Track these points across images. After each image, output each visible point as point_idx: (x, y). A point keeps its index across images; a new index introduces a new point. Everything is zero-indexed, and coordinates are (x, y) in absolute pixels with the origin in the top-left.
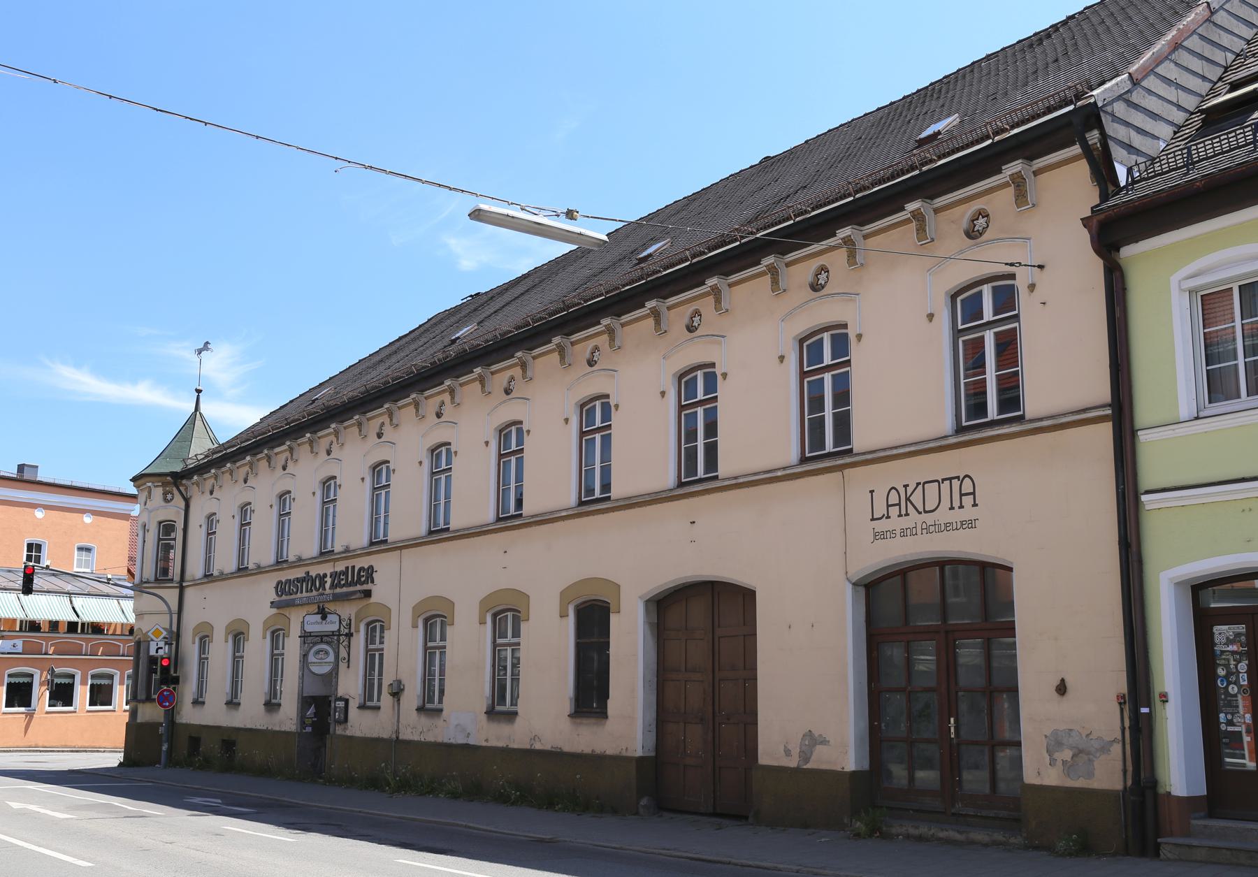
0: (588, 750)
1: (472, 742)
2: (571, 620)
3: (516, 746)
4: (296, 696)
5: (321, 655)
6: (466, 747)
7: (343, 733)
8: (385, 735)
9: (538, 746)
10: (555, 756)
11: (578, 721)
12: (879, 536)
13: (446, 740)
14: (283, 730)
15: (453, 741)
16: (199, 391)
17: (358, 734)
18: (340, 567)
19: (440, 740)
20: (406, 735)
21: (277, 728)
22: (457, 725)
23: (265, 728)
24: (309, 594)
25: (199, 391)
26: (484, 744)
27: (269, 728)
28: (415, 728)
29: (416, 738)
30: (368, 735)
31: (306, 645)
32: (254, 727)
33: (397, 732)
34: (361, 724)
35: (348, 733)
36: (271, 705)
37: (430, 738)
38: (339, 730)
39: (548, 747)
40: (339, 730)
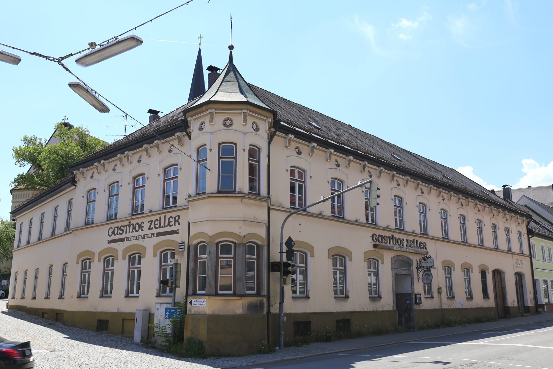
0: (487, 307)
1: (464, 307)
2: (480, 274)
3: (474, 307)
4: (392, 293)
5: (426, 276)
6: (463, 308)
7: (419, 308)
8: (437, 307)
9: (478, 307)
10: (482, 309)
11: (486, 299)
12: (516, 267)
13: (457, 308)
14: (385, 310)
15: (459, 307)
16: (231, 48)
17: (426, 308)
18: (411, 238)
19: (455, 307)
20: (444, 307)
21: (381, 309)
22: (459, 302)
23: (371, 310)
24: (394, 246)
25: (231, 48)
26: (466, 307)
27: (375, 310)
28: (447, 304)
29: (447, 308)
30: (430, 308)
31: (396, 269)
32: (362, 310)
33: (441, 306)
34: (427, 304)
35: (421, 308)
36: (376, 297)
37: (452, 307)
38: (417, 307)
39: (480, 307)
40: (417, 307)
